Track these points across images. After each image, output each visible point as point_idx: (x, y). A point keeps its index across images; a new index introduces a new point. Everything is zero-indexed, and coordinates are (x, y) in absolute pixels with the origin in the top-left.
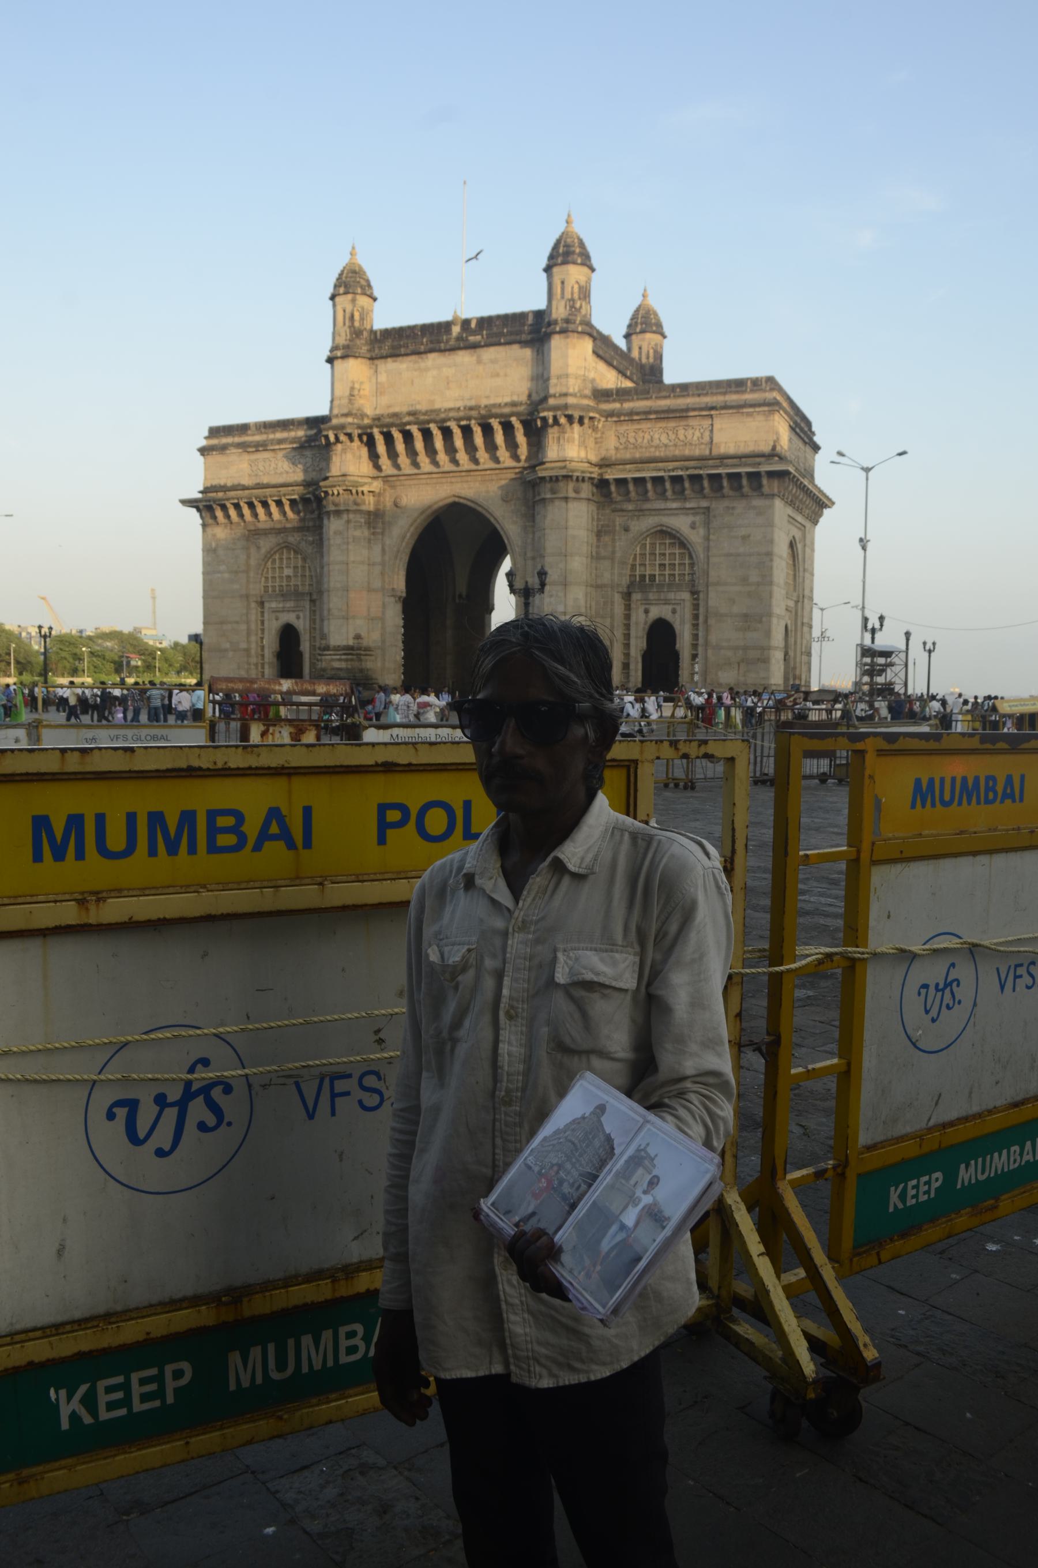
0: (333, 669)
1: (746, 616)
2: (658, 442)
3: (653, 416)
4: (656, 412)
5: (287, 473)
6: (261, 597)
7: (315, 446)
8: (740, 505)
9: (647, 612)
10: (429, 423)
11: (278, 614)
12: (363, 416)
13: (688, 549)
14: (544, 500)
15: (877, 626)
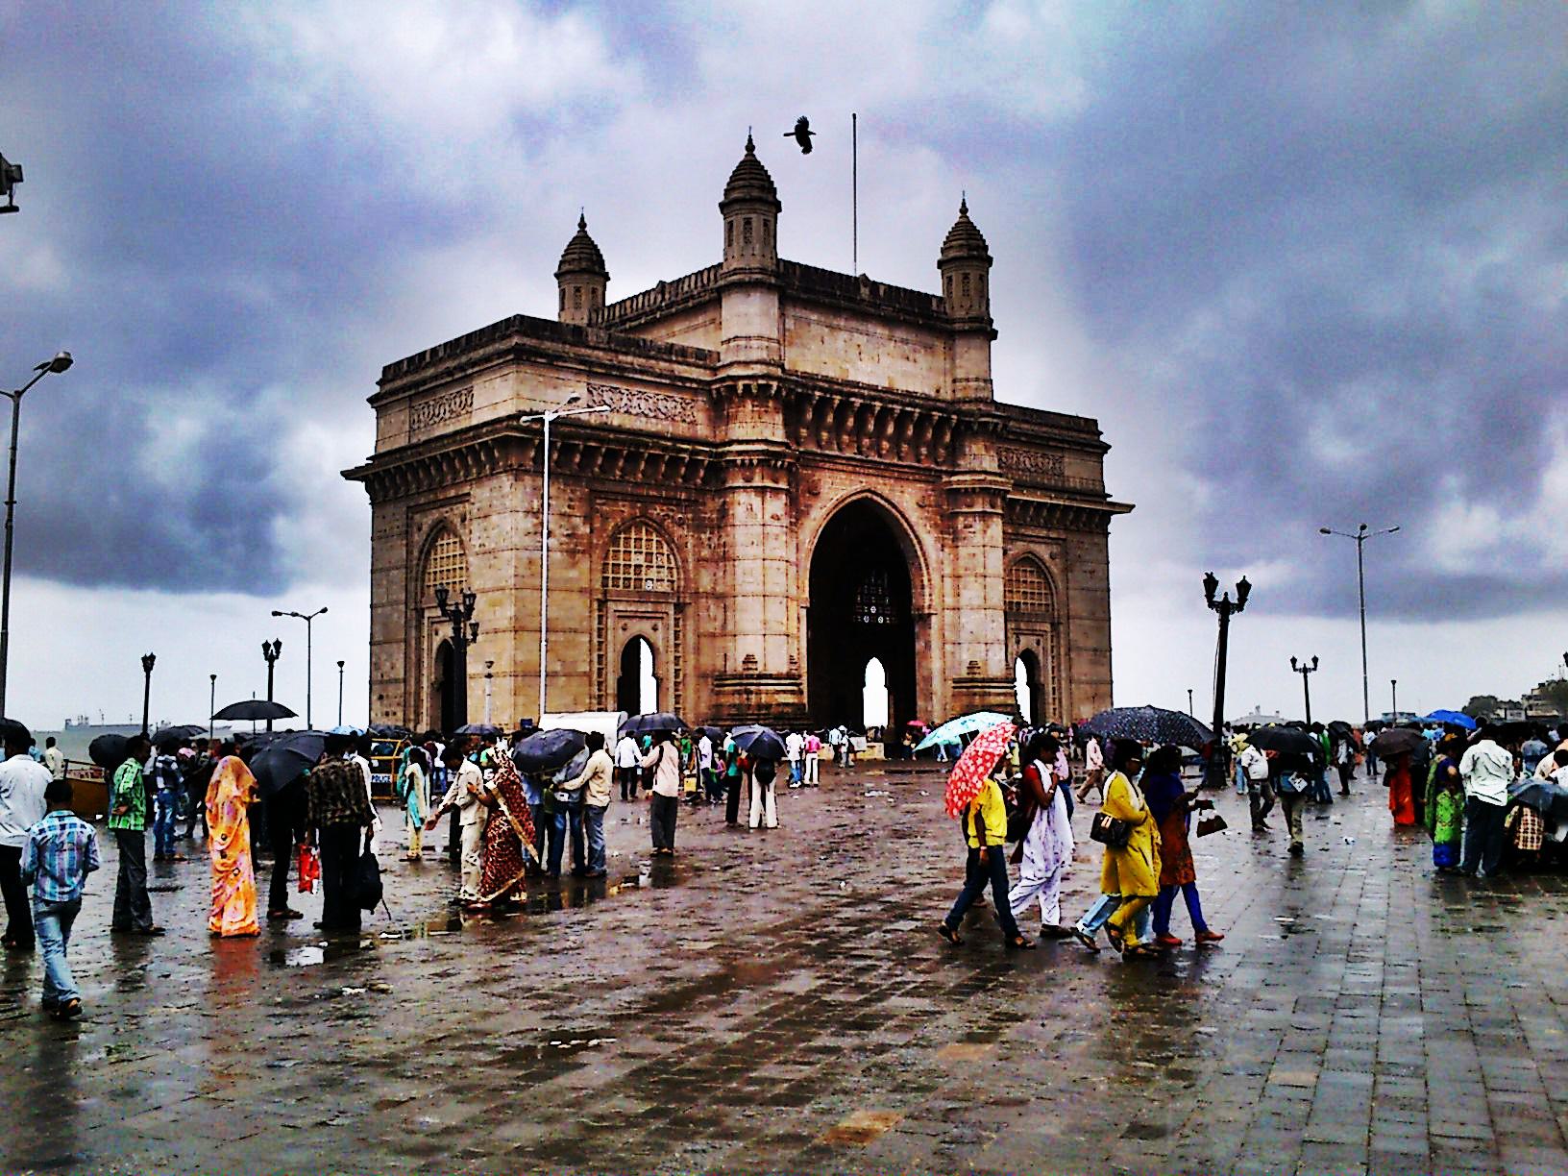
0: (779, 705)
1: (1095, 650)
2: (1022, 466)
3: (1023, 439)
4: (1026, 435)
5: (646, 416)
6: (605, 593)
7: (690, 388)
8: (1087, 540)
9: (1018, 642)
10: (874, 399)
11: (626, 621)
12: (784, 370)
13: (1046, 578)
14: (984, 515)
15: (1310, 665)
